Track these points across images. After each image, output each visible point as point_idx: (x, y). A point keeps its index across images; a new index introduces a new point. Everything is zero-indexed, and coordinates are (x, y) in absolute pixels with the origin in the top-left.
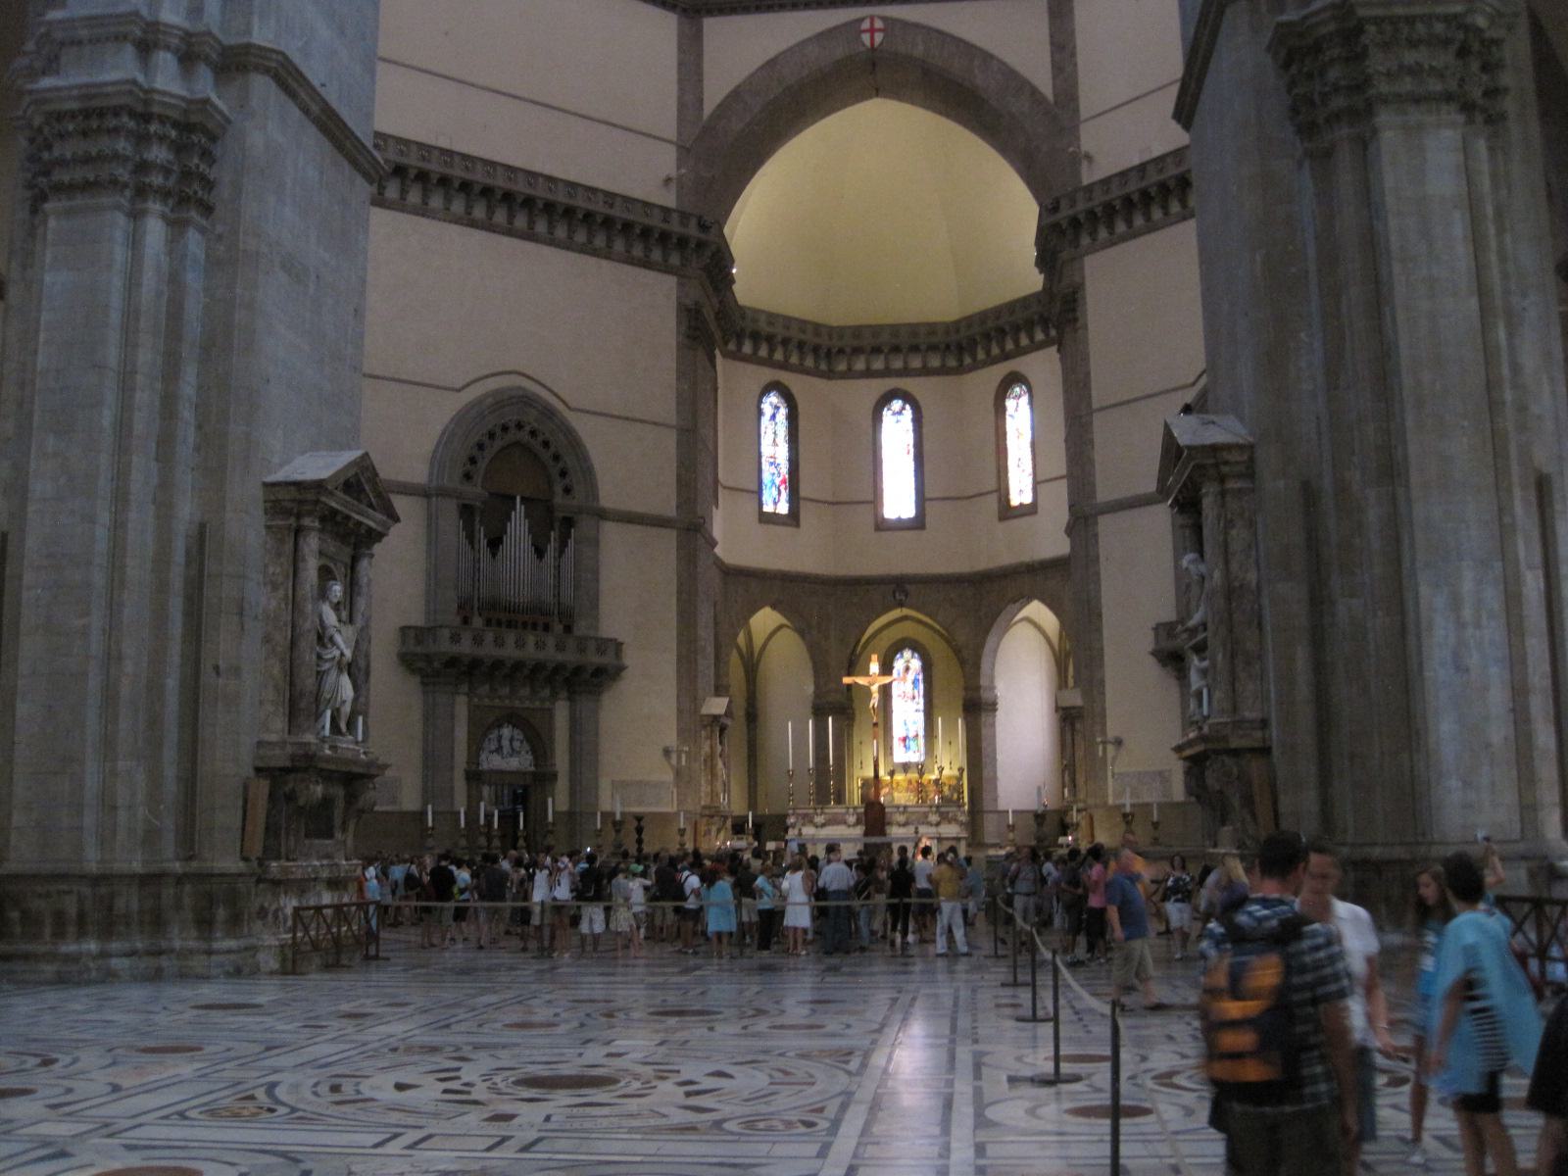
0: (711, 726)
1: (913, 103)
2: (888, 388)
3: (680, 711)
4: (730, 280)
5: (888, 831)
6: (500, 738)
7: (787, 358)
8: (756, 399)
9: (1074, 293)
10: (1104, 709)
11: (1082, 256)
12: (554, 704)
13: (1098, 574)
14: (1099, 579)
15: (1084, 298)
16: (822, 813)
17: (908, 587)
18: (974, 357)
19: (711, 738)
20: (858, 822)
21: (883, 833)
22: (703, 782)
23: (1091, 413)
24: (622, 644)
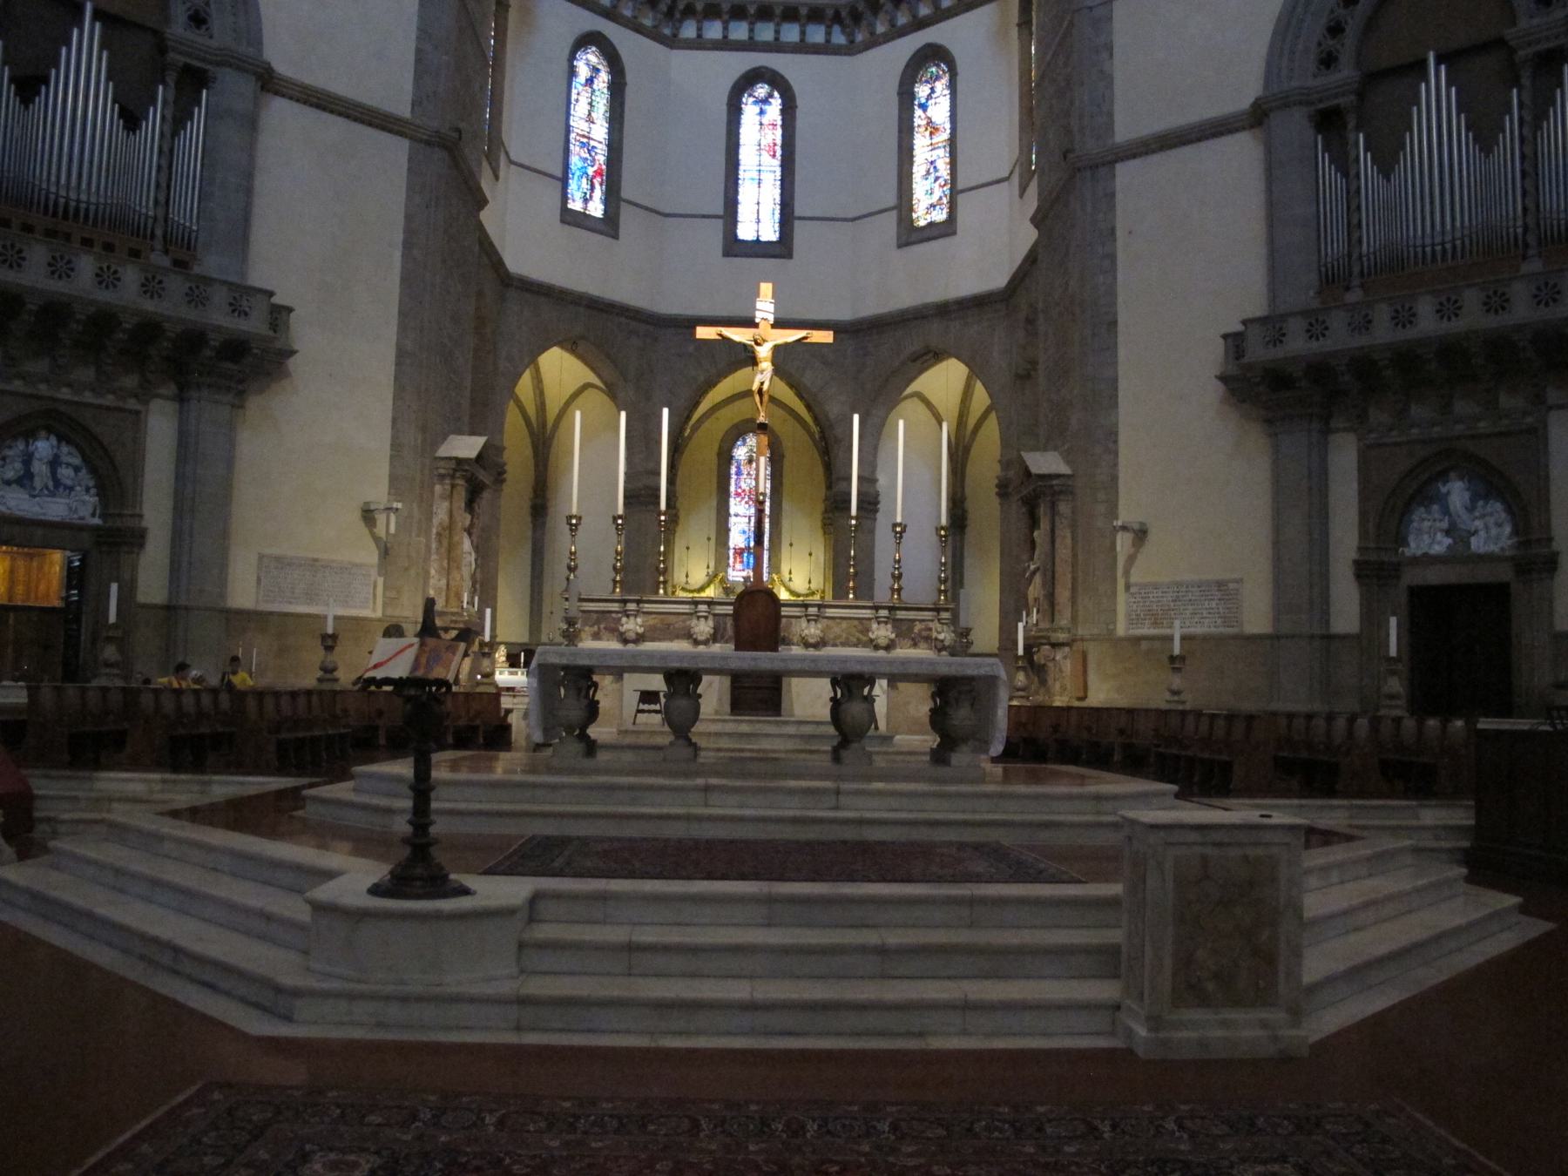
0: (453, 477)
2: (747, 67)
3: (396, 446)
6: (28, 459)
8: (567, 52)
10: (1114, 479)
12: (146, 403)
13: (1112, 257)
16: (637, 613)
19: (451, 496)
20: (715, 637)
22: (433, 572)
24: (290, 310)
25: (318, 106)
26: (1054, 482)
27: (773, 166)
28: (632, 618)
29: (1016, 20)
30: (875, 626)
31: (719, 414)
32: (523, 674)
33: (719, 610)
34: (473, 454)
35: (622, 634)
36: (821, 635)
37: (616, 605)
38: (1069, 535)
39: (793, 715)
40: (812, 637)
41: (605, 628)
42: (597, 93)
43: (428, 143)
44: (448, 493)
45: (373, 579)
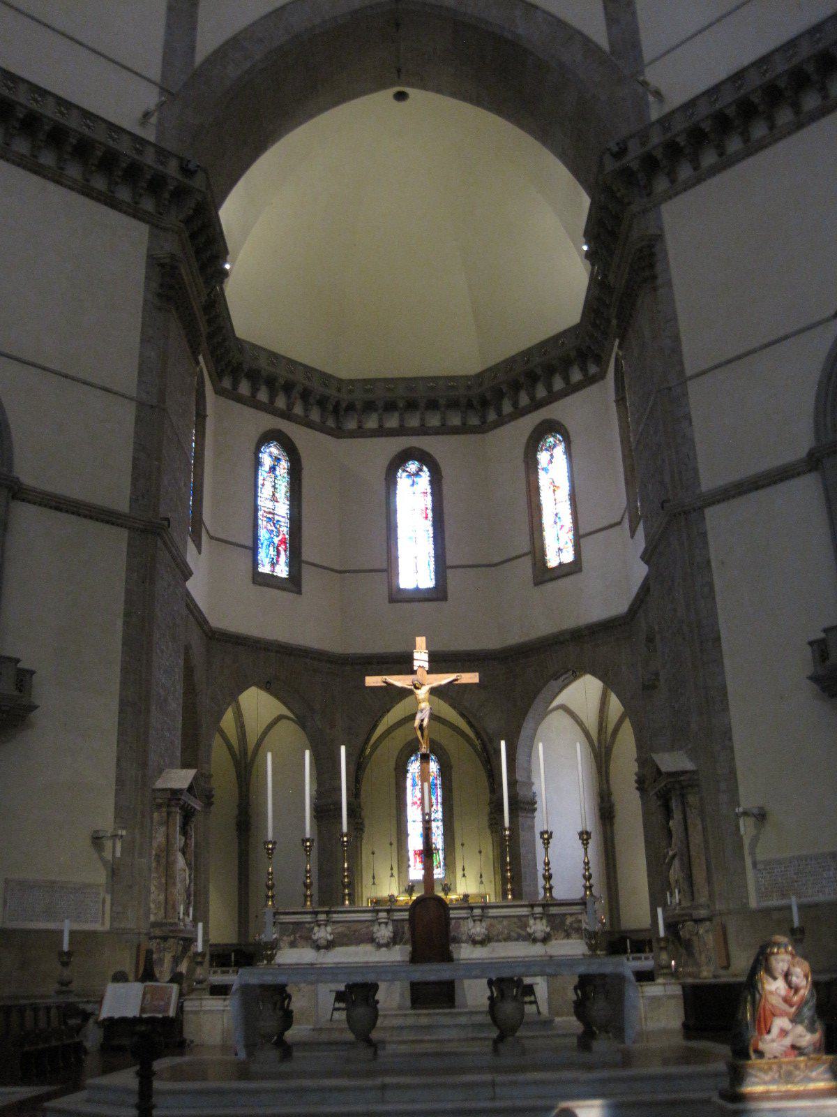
0: (168, 806)
1: (439, 91)
2: (399, 449)
3: (120, 782)
4: (225, 274)
5: (455, 956)
7: (290, 406)
8: (253, 448)
9: (651, 247)
10: (733, 773)
11: (657, 206)
13: (711, 586)
14: (712, 589)
15: (665, 251)
16: (326, 924)
18: (499, 413)
19: (167, 823)
20: (395, 940)
21: (448, 958)
22: (153, 889)
23: (683, 380)
24: (32, 673)
25: (57, 509)
26: (682, 778)
27: (427, 528)
28: (323, 927)
29: (613, 398)
30: (531, 922)
31: (392, 735)
33: (397, 916)
34: (185, 785)
35: (315, 941)
36: (486, 932)
39: (466, 1006)
40: (478, 935)
41: (300, 937)
42: (279, 478)
43: (143, 531)
44: (166, 818)
45: (101, 897)
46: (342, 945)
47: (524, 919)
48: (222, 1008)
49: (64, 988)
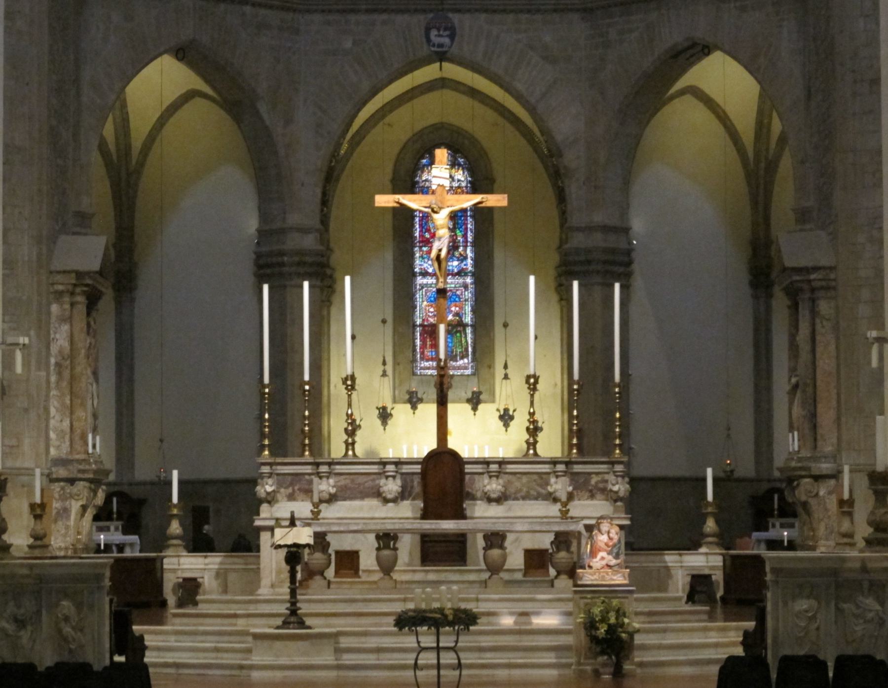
0: (72, 294)
5: (468, 513)
16: (329, 475)
17: (455, 18)
19: (70, 319)
20: (403, 495)
22: (53, 411)
26: (812, 277)
28: (325, 479)
30: (553, 480)
31: (391, 118)
32: (117, 529)
33: (406, 469)
36: (503, 490)
37: (309, 467)
38: (833, 341)
40: (494, 491)
41: (299, 489)
44: (67, 313)
46: (345, 499)
47: (544, 476)
48: (202, 567)
49: (39, 543)
